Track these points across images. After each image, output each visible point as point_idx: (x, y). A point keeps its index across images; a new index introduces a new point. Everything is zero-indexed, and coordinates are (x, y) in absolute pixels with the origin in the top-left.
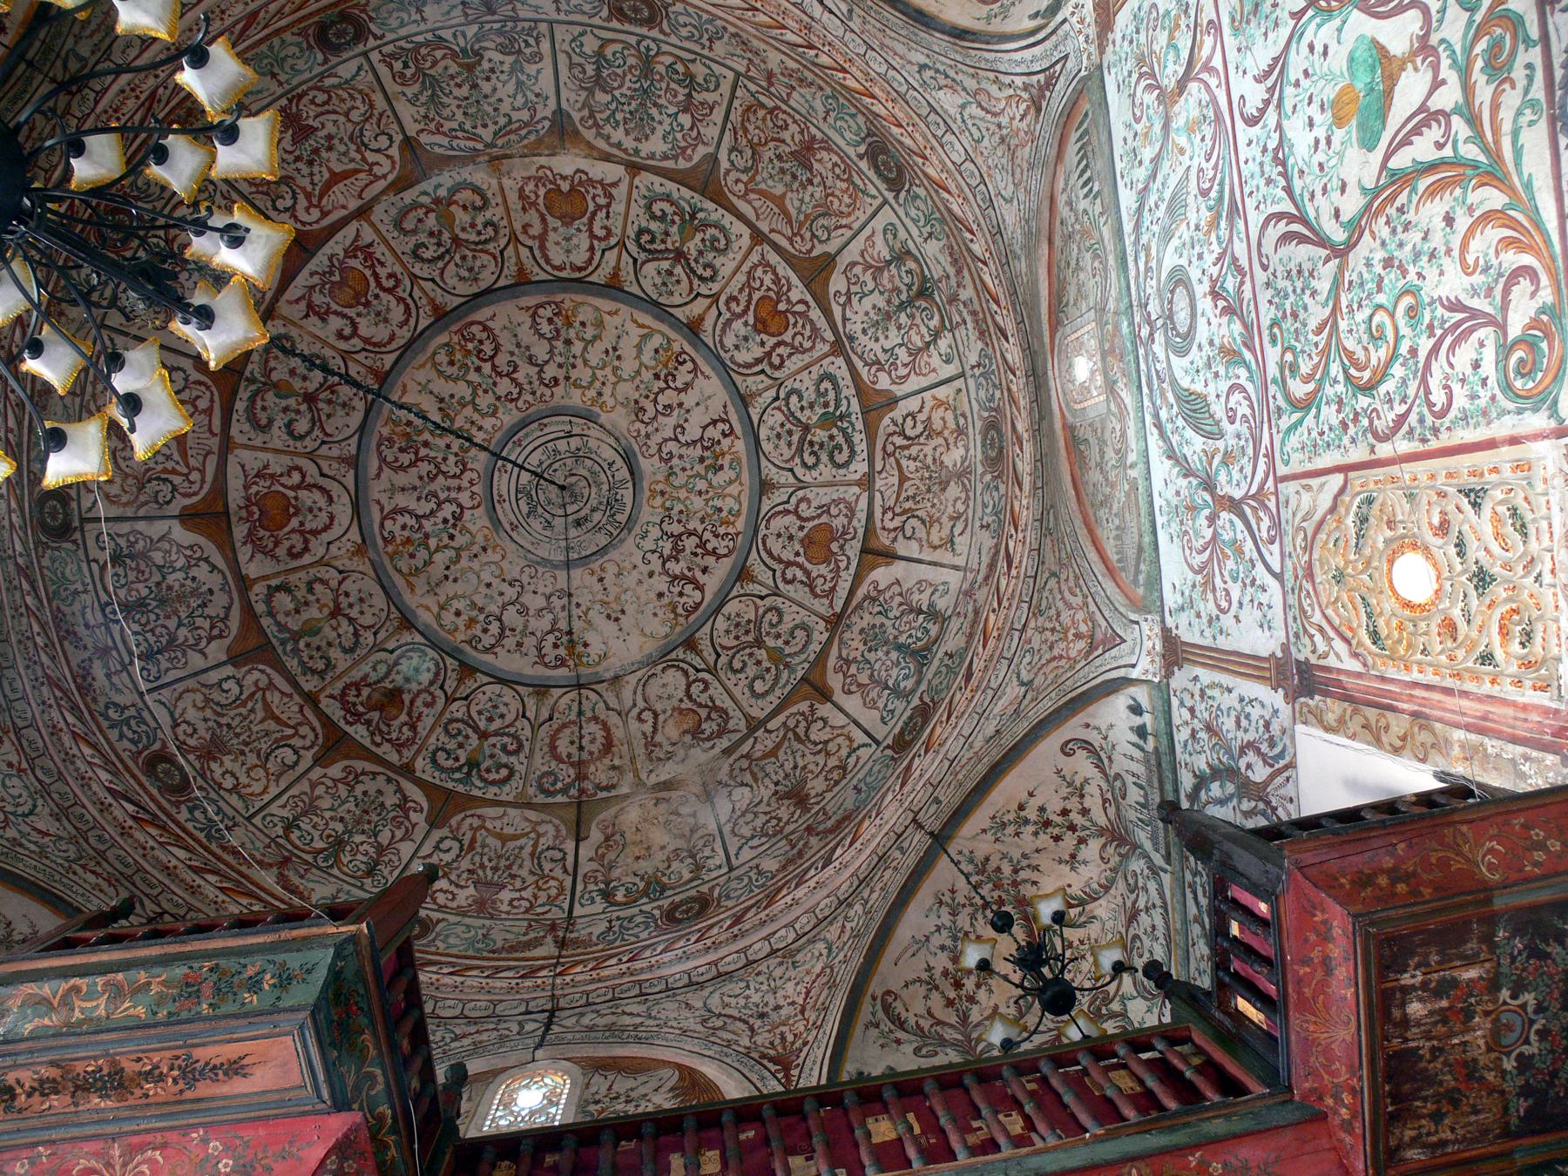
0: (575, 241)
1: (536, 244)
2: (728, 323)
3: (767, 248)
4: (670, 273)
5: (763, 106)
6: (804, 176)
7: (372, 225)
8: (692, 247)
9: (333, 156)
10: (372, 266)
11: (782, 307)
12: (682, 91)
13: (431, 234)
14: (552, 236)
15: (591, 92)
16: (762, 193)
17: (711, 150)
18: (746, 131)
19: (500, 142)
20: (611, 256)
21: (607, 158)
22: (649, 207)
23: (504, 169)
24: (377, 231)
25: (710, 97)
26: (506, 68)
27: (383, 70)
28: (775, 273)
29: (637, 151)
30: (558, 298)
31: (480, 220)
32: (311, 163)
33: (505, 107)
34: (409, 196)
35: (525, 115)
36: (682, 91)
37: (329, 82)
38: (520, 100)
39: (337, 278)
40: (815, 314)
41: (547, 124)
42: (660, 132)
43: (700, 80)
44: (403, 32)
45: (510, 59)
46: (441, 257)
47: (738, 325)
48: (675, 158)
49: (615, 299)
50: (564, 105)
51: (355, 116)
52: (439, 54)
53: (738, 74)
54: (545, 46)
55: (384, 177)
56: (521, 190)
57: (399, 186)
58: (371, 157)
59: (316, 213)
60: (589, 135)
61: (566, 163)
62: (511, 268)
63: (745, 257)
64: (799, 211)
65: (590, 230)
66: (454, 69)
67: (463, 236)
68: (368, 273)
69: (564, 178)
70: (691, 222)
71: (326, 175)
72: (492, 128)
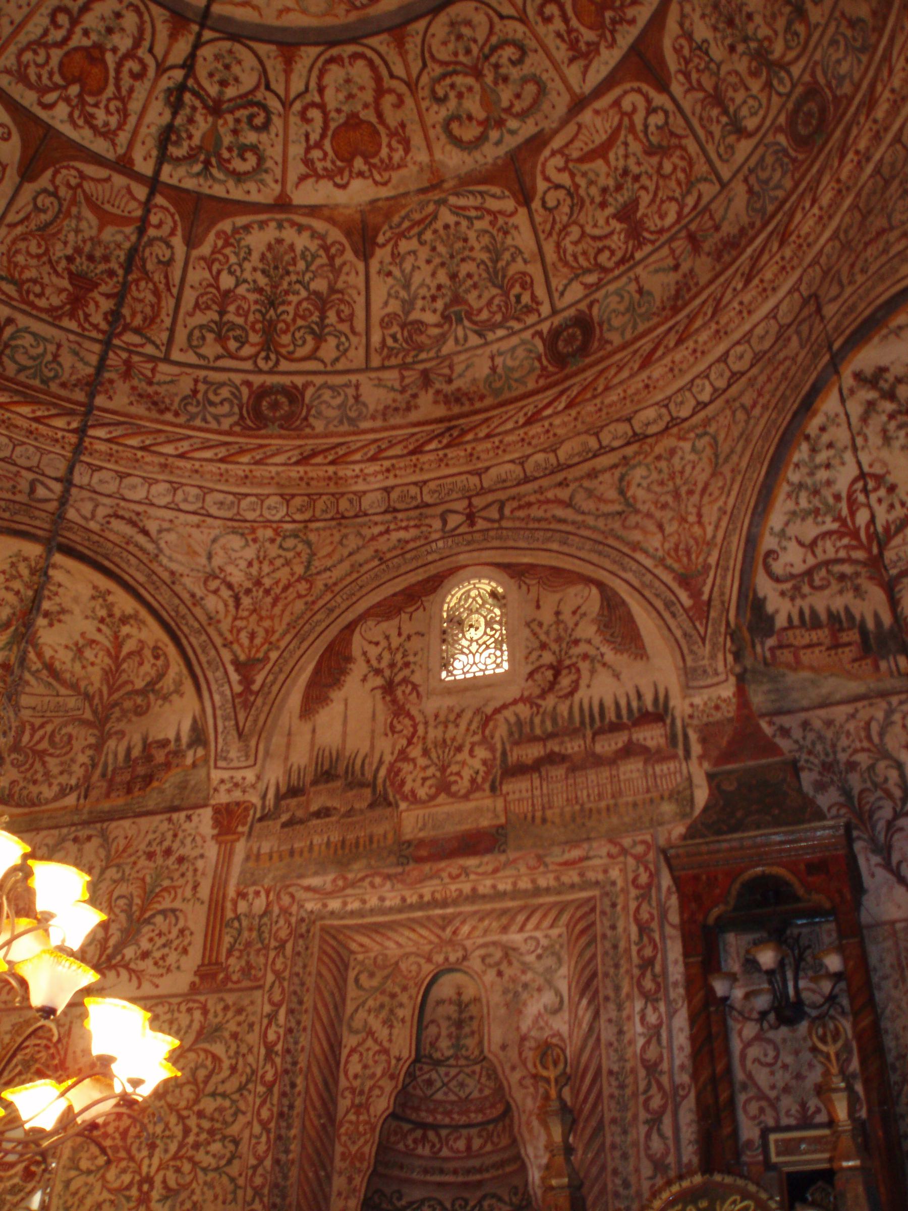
0: (341, 96)
1: (388, 83)
2: (137, 44)
3: (111, 156)
4: (223, 83)
5: (137, 331)
6: (81, 265)
7: (569, 88)
8: (202, 124)
9: (602, 181)
10: (570, 31)
11: (74, 90)
12: (231, 317)
13: (506, 79)
14: (368, 96)
15: (332, 290)
16: (124, 221)
17: (195, 253)
18: (156, 293)
19: (431, 208)
20: (297, 86)
21: (313, 210)
22: (261, 160)
23: (427, 175)
24: (564, 80)
25: (201, 318)
26: (419, 303)
27: (541, 292)
28: (93, 128)
29: (280, 226)
30: (353, 16)
31: (452, 103)
32: (626, 172)
33: (424, 253)
34: (528, 129)
35: (404, 246)
36: (231, 317)
37: (591, 279)
38: (410, 261)
39: (608, 14)
40: (28, 98)
41: (381, 239)
42: (255, 256)
43: (210, 337)
44: (515, 340)
45: (415, 315)
46: (494, 49)
47: (124, 43)
48: (236, 231)
49: (284, 30)
50: (361, 266)
51: (575, 231)
52: (485, 315)
53: (167, 360)
54: (376, 338)
55: (553, 154)
56: (407, 151)
57: (538, 142)
58: (564, 179)
59: (626, 105)
60: (335, 235)
61: (359, 193)
62: (413, 46)
63: (135, 133)
64: (79, 218)
65: (325, 114)
66: (472, 297)
67: (470, 81)
68: (574, 23)
69: (361, 174)
70: (208, 156)
71: (611, 156)
72: (439, 225)
